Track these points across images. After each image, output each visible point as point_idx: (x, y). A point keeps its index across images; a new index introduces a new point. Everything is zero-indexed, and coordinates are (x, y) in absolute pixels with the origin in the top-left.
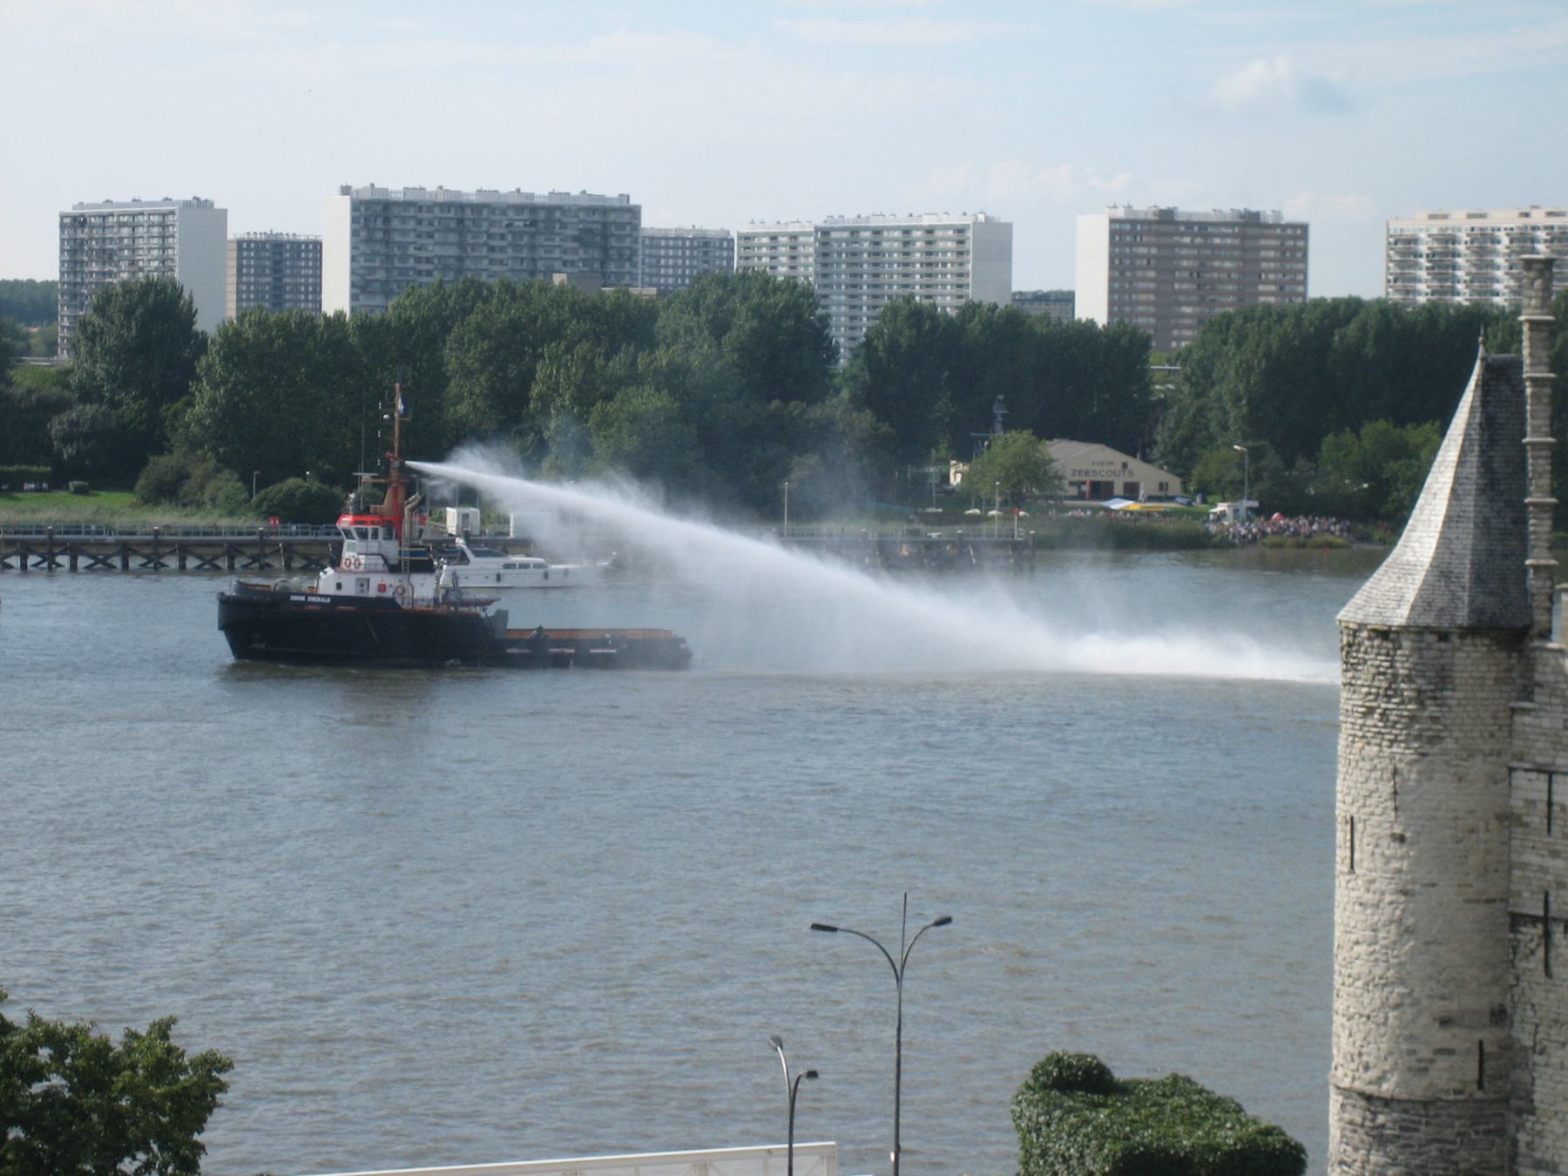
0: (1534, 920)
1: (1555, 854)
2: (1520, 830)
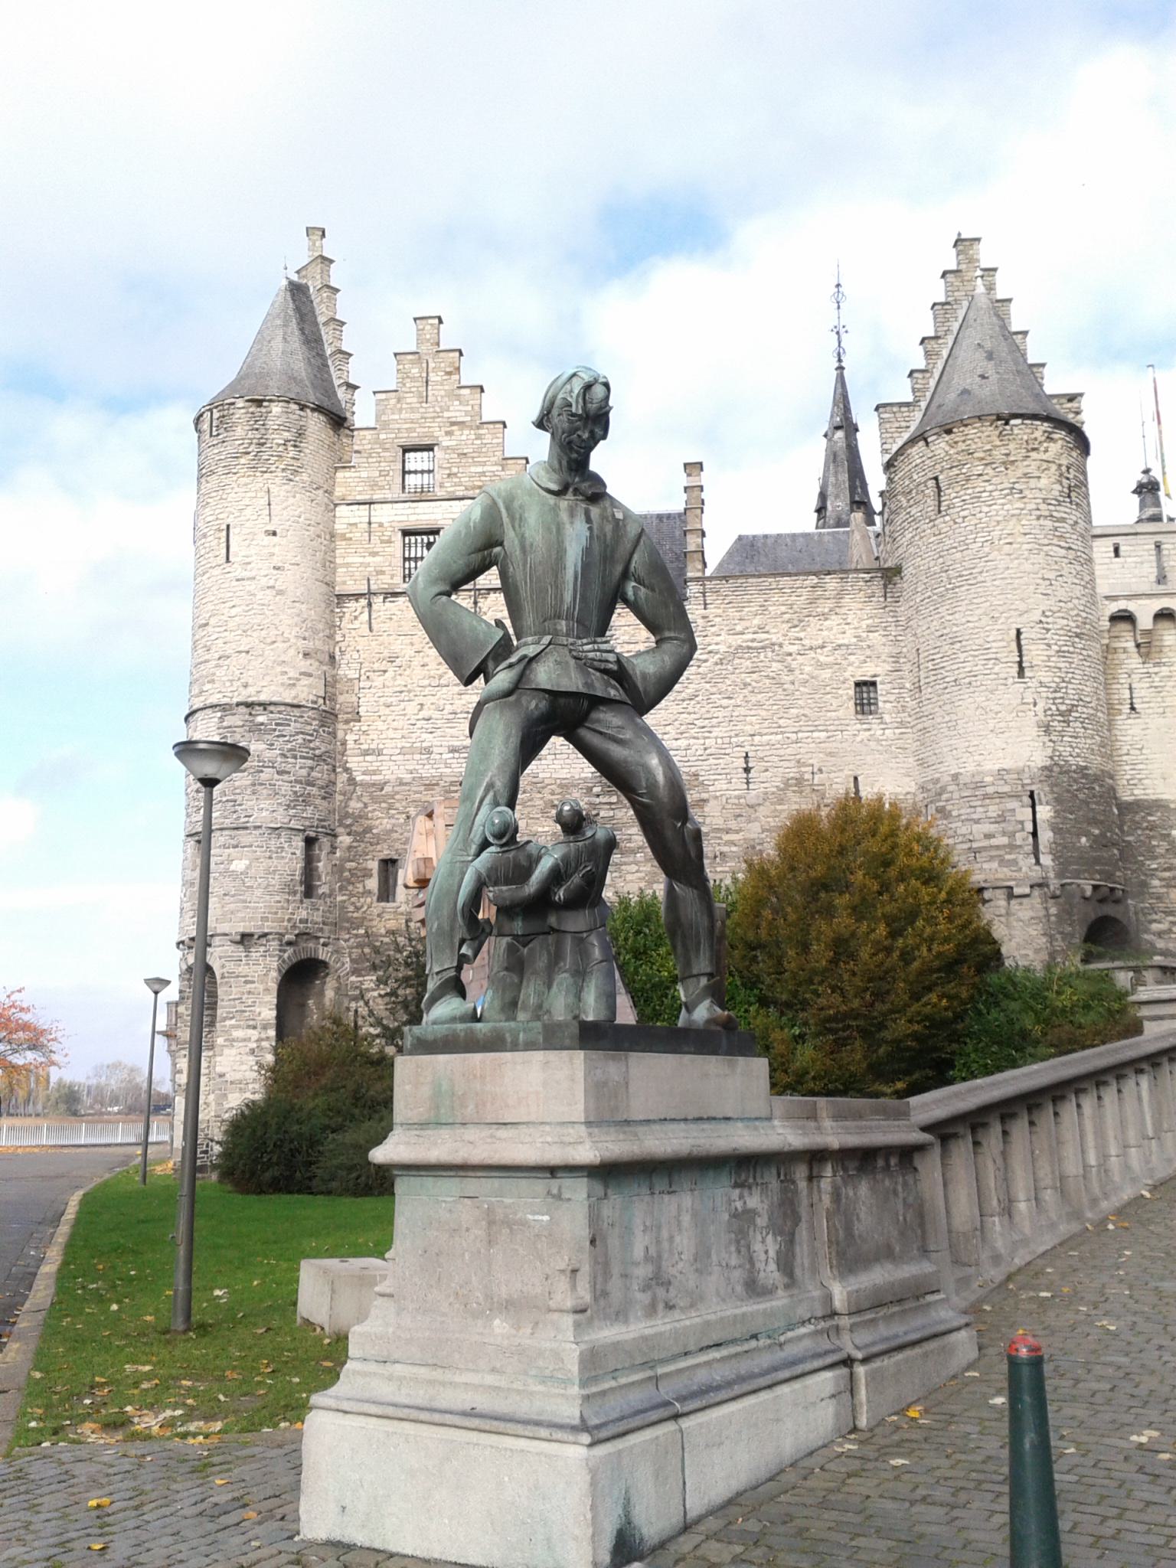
0: (357, 596)
1: (374, 554)
2: (344, 543)
